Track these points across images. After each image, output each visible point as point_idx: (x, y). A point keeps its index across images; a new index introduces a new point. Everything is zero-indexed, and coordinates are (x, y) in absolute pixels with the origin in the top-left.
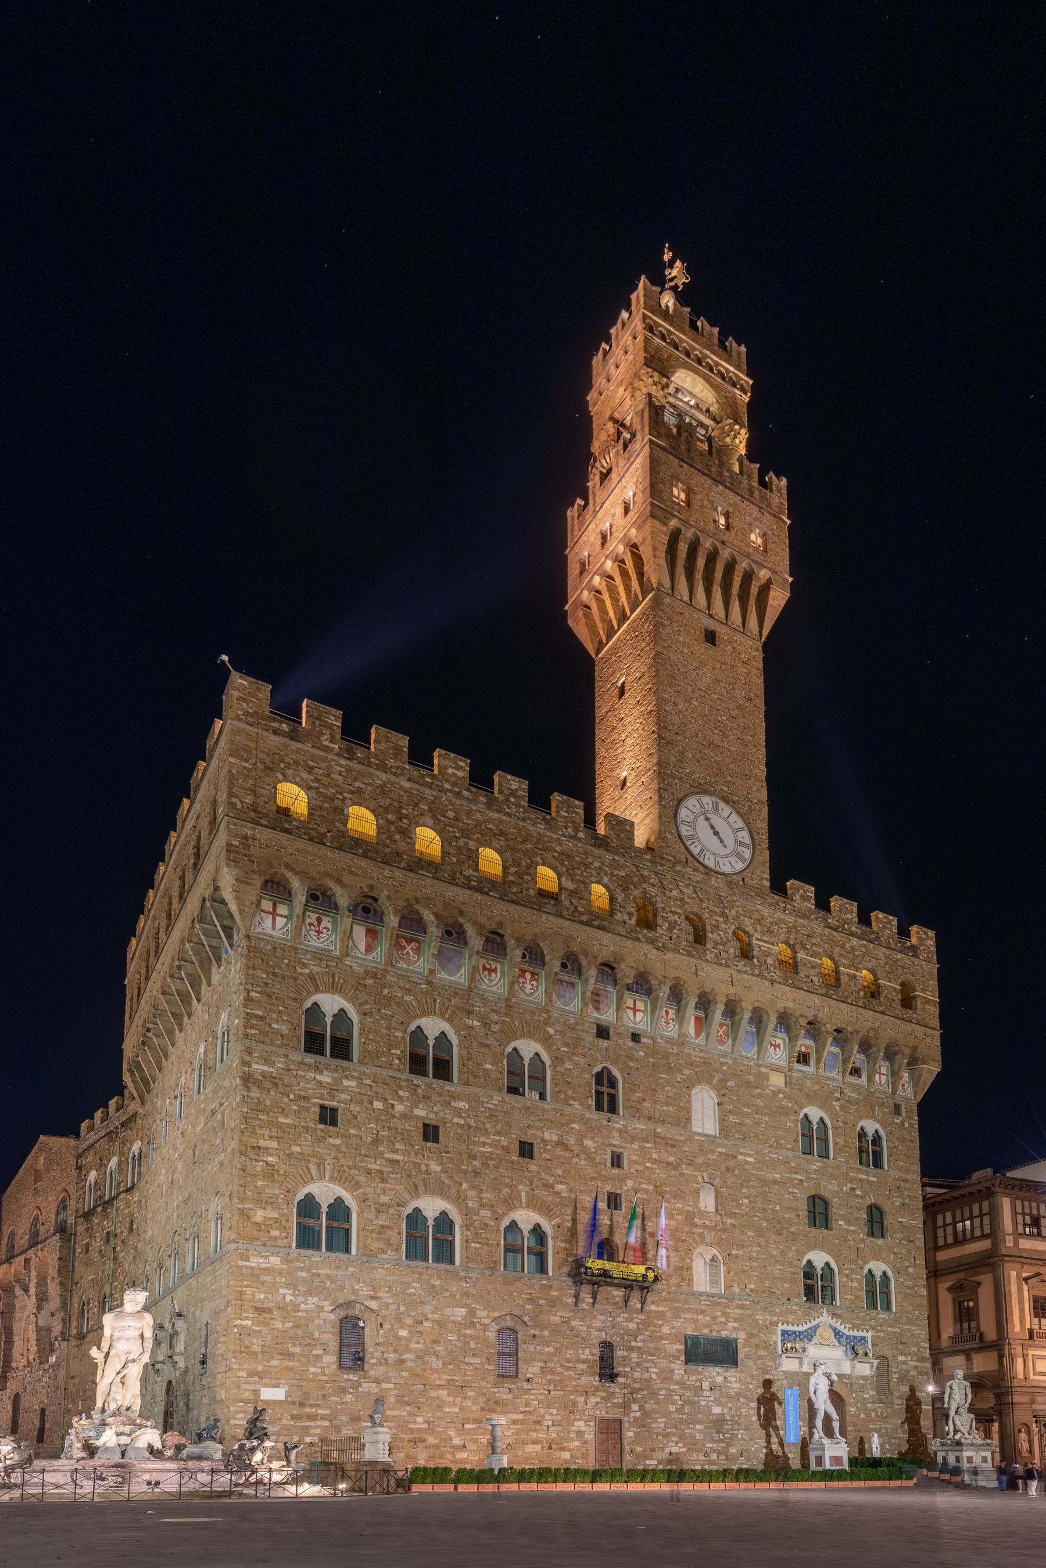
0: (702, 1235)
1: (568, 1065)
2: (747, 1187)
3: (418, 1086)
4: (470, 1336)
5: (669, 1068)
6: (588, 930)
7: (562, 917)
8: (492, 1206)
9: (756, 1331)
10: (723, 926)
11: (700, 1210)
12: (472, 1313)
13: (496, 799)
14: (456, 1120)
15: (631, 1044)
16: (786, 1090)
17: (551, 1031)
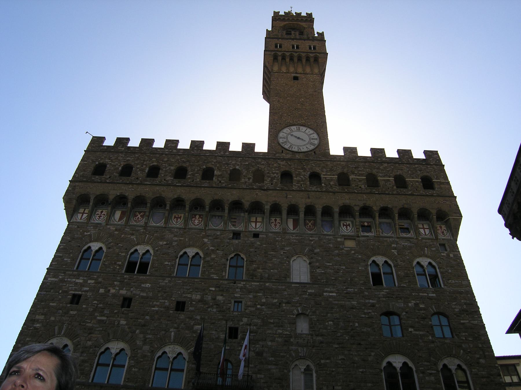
3: (126, 278)
15: (253, 239)
17: (206, 240)
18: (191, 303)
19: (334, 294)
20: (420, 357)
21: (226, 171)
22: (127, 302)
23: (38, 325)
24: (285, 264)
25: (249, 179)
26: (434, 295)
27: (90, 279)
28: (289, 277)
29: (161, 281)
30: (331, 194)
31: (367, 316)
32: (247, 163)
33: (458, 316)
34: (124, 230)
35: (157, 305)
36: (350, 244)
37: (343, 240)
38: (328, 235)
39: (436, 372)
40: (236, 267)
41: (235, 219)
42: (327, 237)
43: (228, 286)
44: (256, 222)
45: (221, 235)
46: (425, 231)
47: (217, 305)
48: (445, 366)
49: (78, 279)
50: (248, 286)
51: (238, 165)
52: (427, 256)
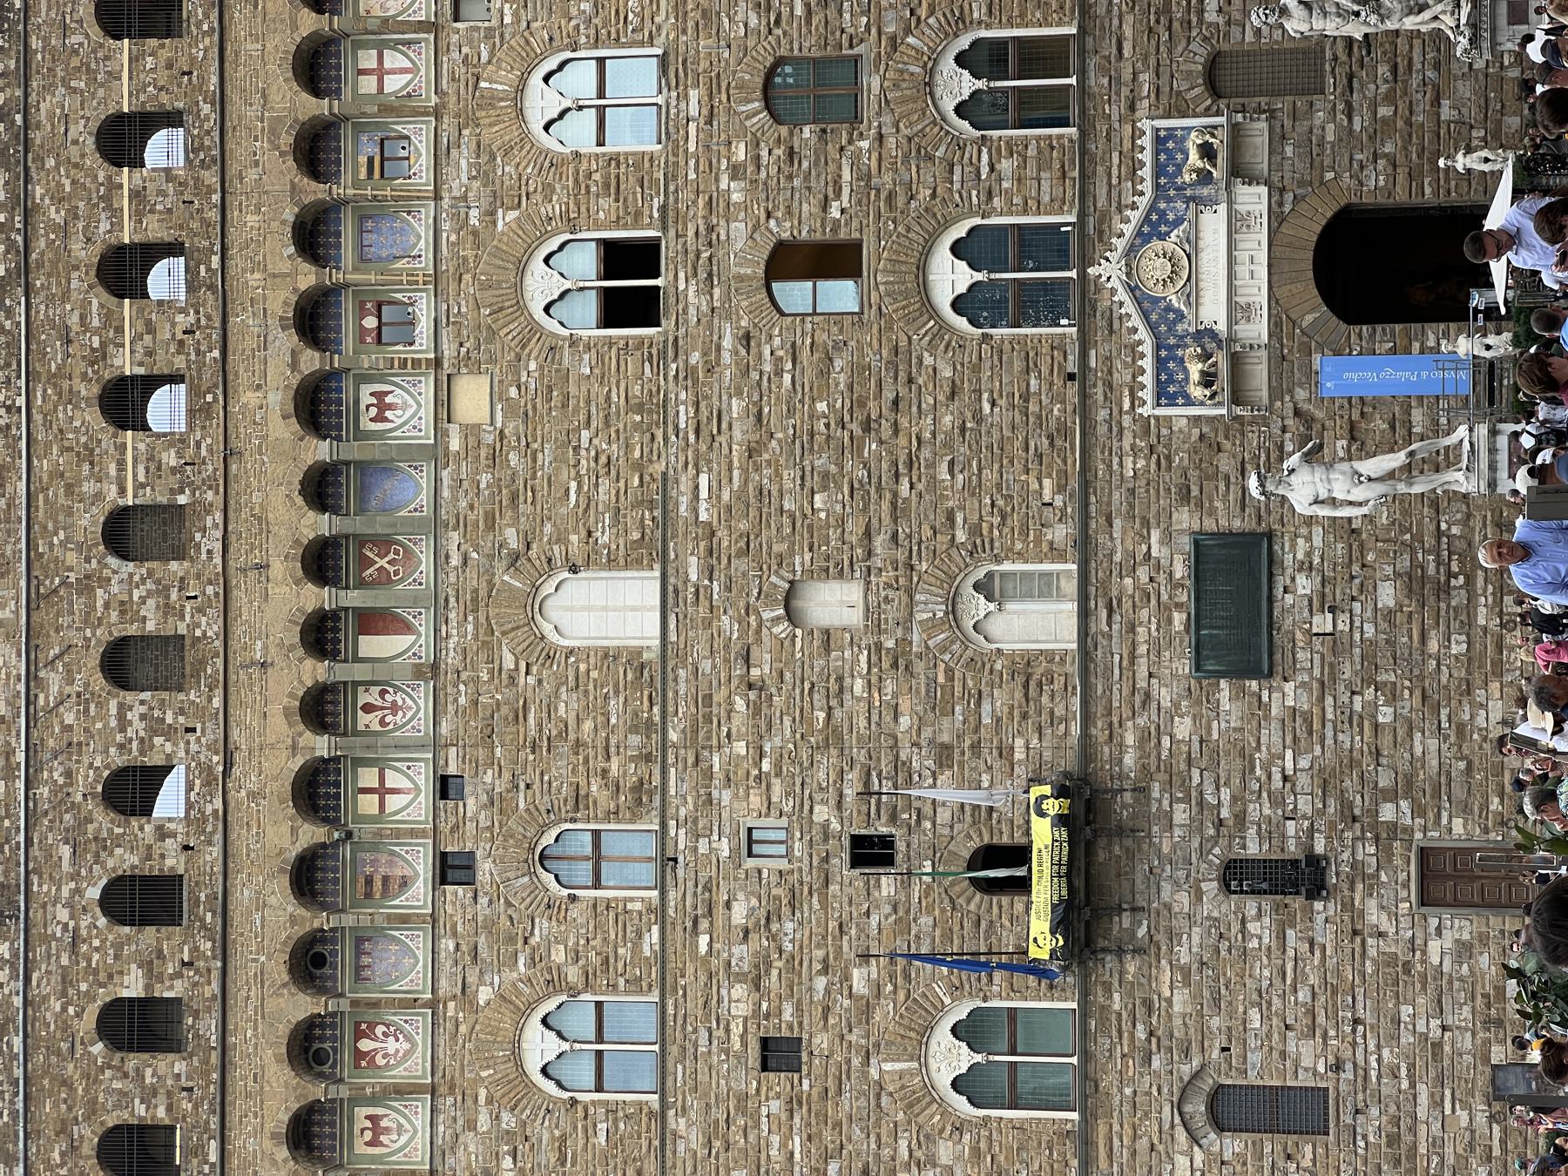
15: (470, 802)
18: (767, 1016)
19: (703, 480)
20: (934, 195)
21: (118, 947)
24: (583, 667)
25: (162, 833)
26: (694, 94)
28: (639, 652)
29: (681, 1147)
30: (234, 468)
31: (789, 366)
32: (66, 851)
33: (778, 22)
35: (783, 1145)
36: (473, 398)
37: (454, 429)
39: (985, 150)
40: (597, 857)
41: (369, 881)
42: (446, 493)
43: (690, 884)
44: (382, 791)
45: (455, 934)
46: (400, 72)
47: (768, 919)
50: (683, 812)
51: (78, 891)
52: (521, 88)
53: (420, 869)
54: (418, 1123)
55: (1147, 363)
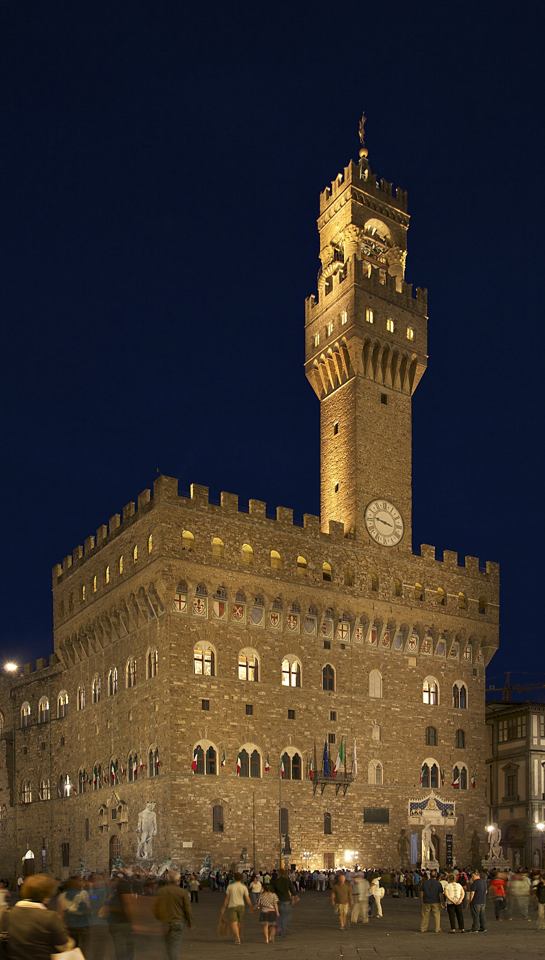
0: (373, 753)
1: (311, 666)
2: (396, 725)
4: (267, 813)
5: (358, 662)
6: (321, 591)
7: (309, 586)
8: (276, 746)
9: (398, 804)
10: (387, 578)
11: (372, 740)
12: (268, 801)
13: (278, 523)
14: (260, 702)
15: (340, 650)
16: (417, 667)
22: (249, 709)
23: (183, 730)
26: (461, 715)
27: (213, 684)
34: (228, 628)
36: (412, 662)
38: (397, 651)
41: (324, 624)
44: (342, 631)
48: (456, 767)
49: (202, 683)
52: (463, 679)
53: (327, 637)
54: (276, 628)
55: (417, 801)
